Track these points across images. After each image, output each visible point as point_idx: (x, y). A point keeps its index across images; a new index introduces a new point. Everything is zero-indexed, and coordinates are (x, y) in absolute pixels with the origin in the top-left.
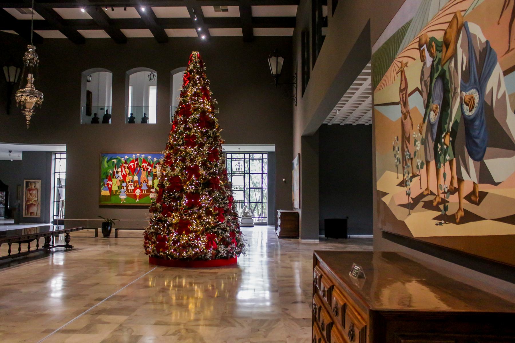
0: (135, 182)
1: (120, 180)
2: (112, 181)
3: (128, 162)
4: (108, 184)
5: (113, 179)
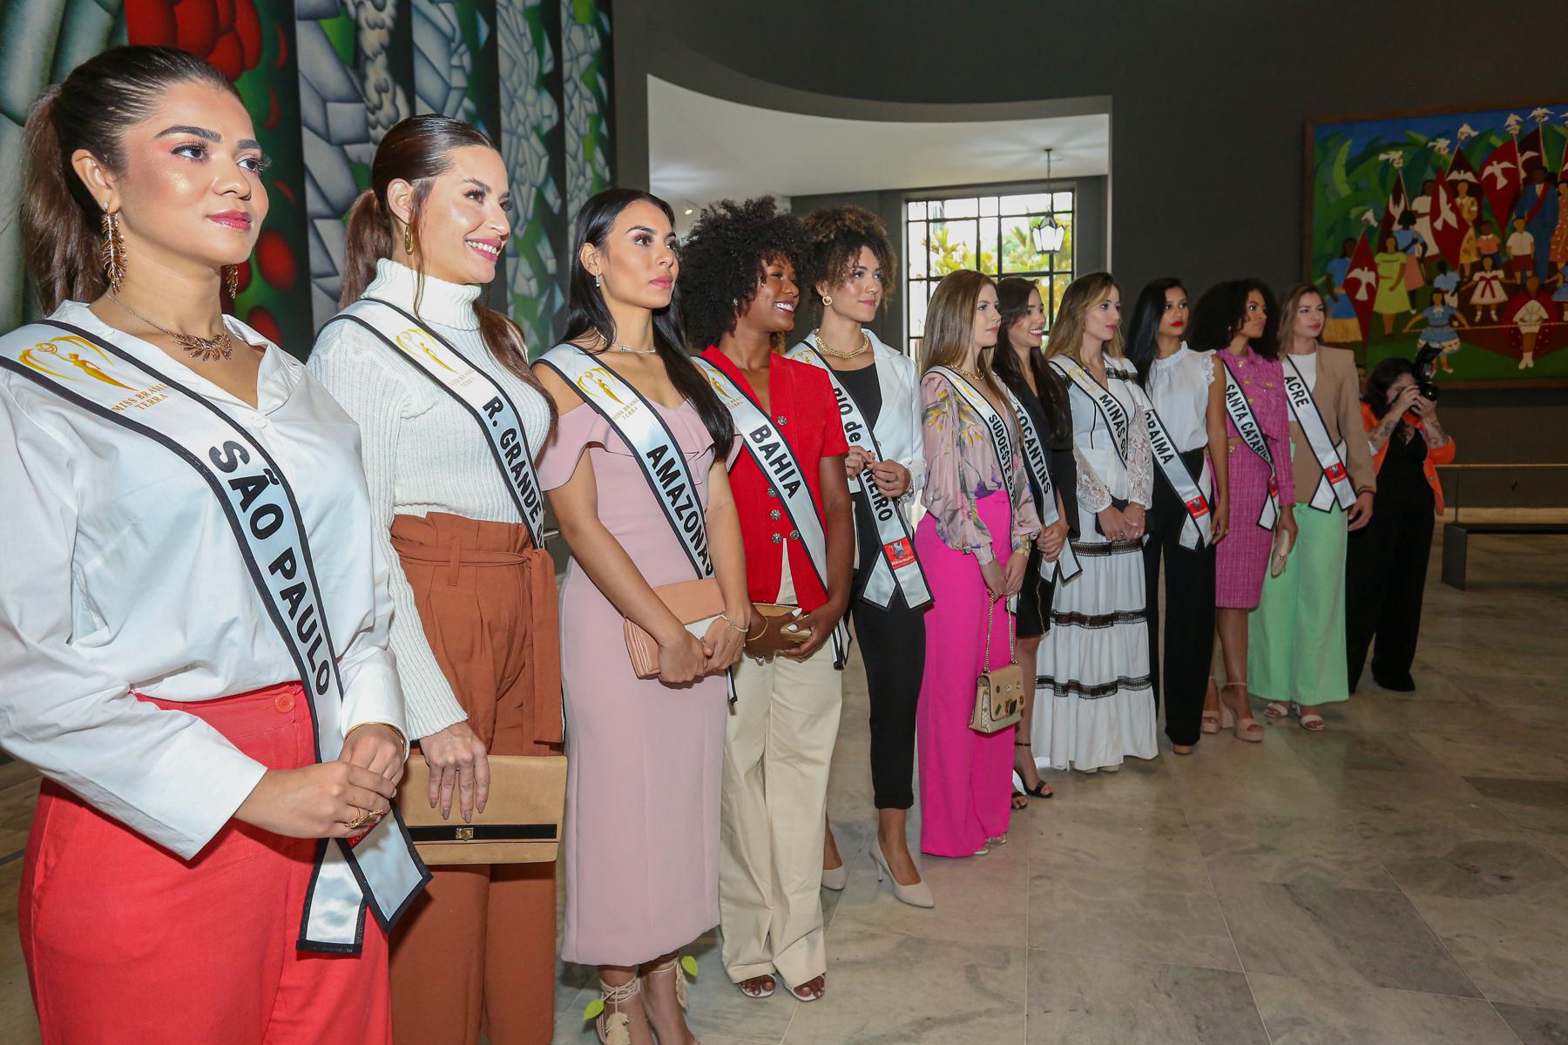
0: (1512, 265)
1: (1422, 260)
2: (1373, 267)
3: (1475, 161)
4: (1353, 285)
5: (1379, 258)
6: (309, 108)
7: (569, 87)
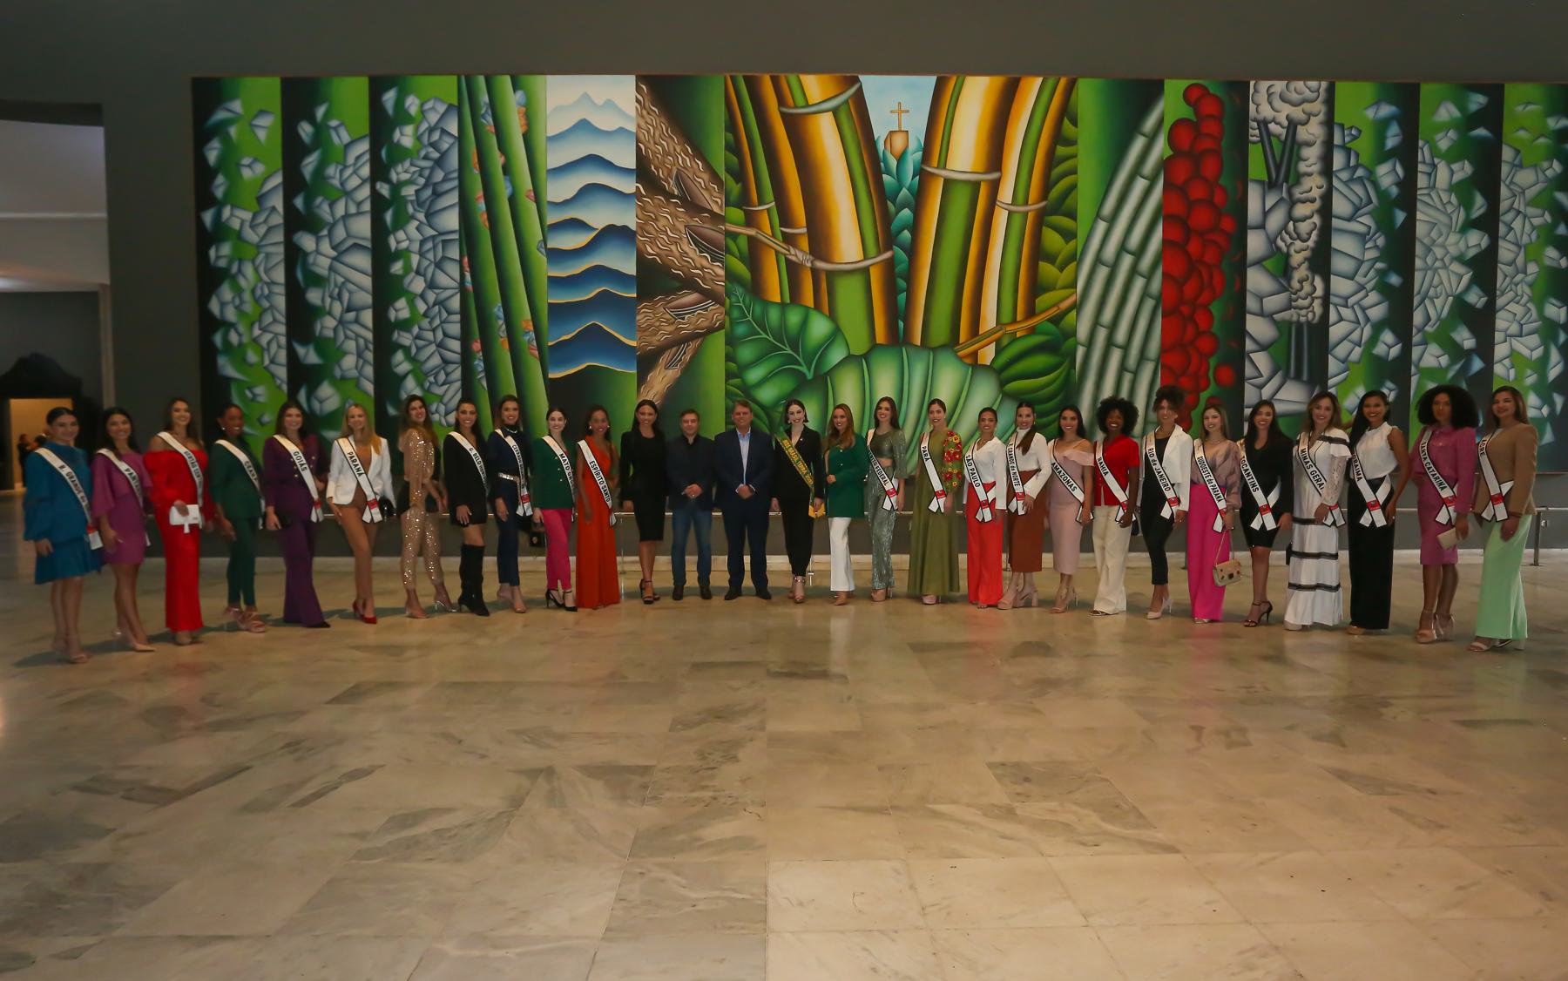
6: (1251, 303)
7: (1508, 218)
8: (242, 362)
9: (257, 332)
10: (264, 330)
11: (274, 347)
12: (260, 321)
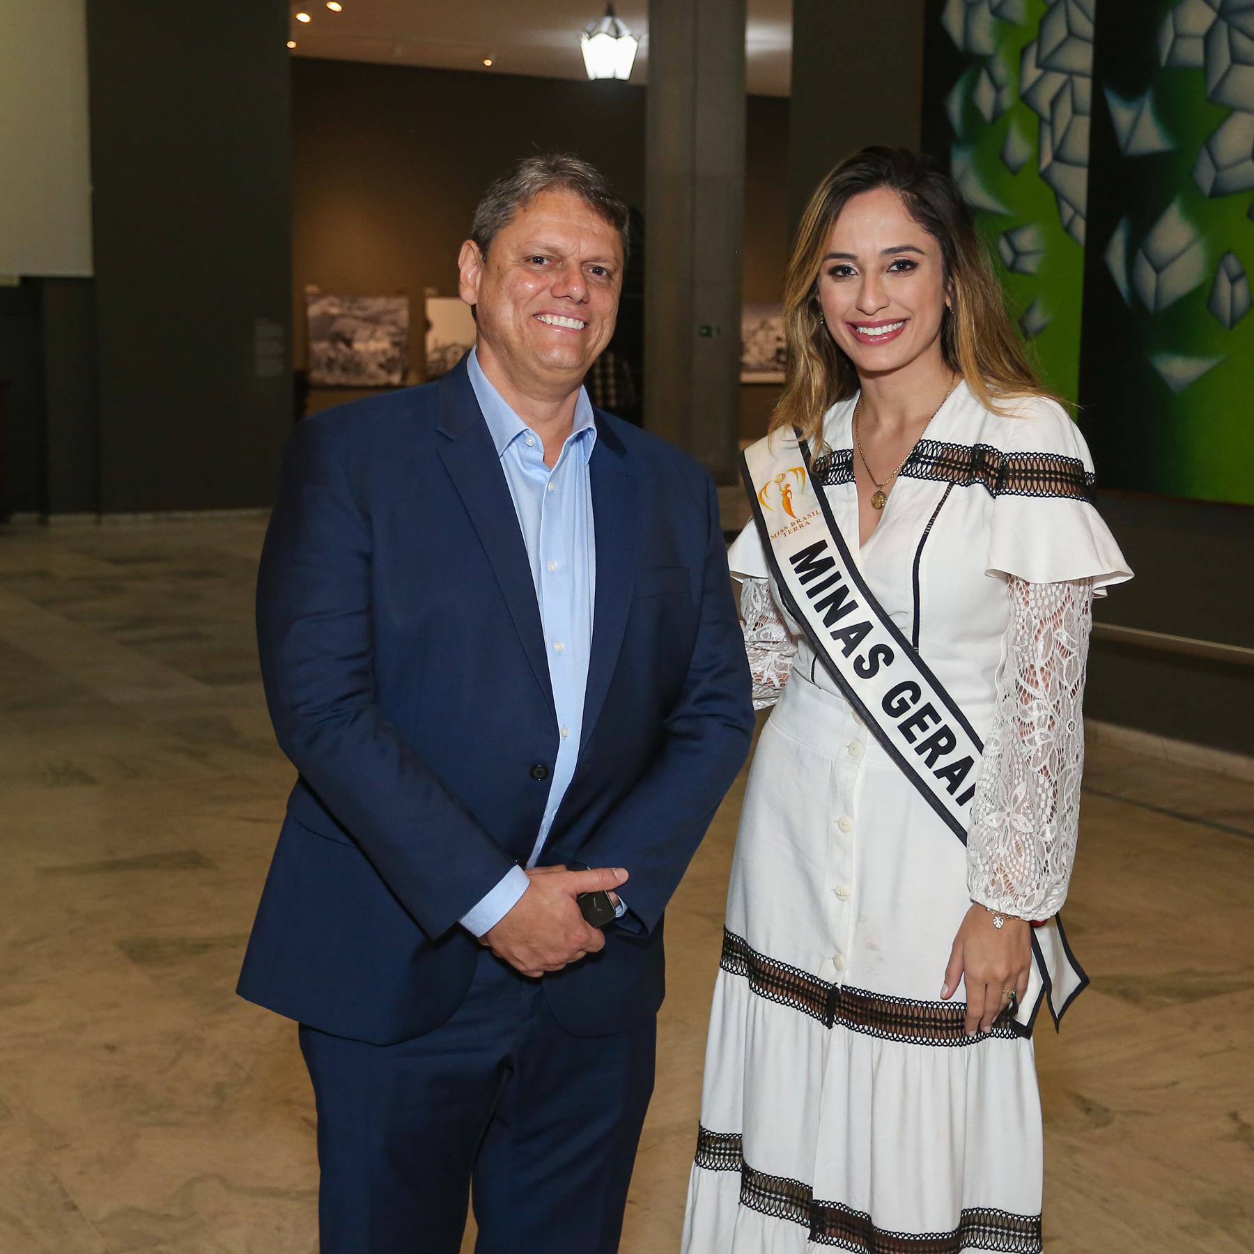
8: (997, 166)
9: (1032, 73)
10: (1045, 65)
11: (1065, 109)
12: (1039, 39)
